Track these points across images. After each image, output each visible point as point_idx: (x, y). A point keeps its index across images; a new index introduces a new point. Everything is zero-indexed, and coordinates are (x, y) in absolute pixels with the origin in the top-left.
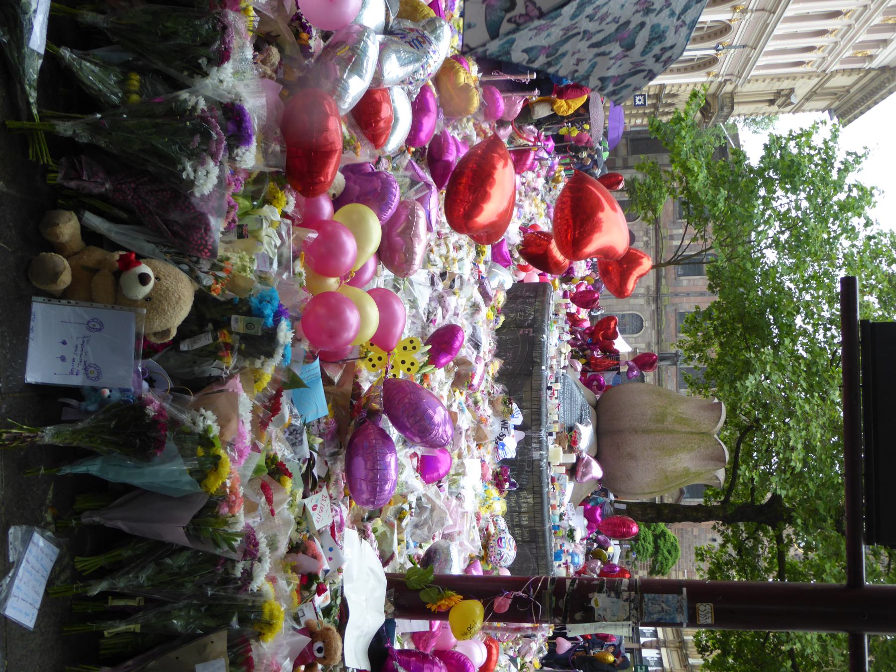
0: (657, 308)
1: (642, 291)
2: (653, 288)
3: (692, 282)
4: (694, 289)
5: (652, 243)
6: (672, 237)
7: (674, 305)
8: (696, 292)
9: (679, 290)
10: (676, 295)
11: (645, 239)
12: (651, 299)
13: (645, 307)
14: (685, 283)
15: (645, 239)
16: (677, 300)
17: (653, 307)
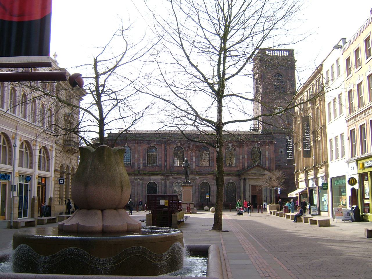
0: (171, 175)
1: (163, 182)
2: (162, 177)
3: (160, 160)
4: (163, 159)
5: (141, 177)
6: (139, 168)
7: (170, 168)
8: (165, 158)
9: (163, 165)
10: (165, 166)
11: (139, 180)
12: (167, 178)
13: (171, 181)
14: (160, 163)
15: (139, 180)
16: (168, 167)
17: (171, 177)
